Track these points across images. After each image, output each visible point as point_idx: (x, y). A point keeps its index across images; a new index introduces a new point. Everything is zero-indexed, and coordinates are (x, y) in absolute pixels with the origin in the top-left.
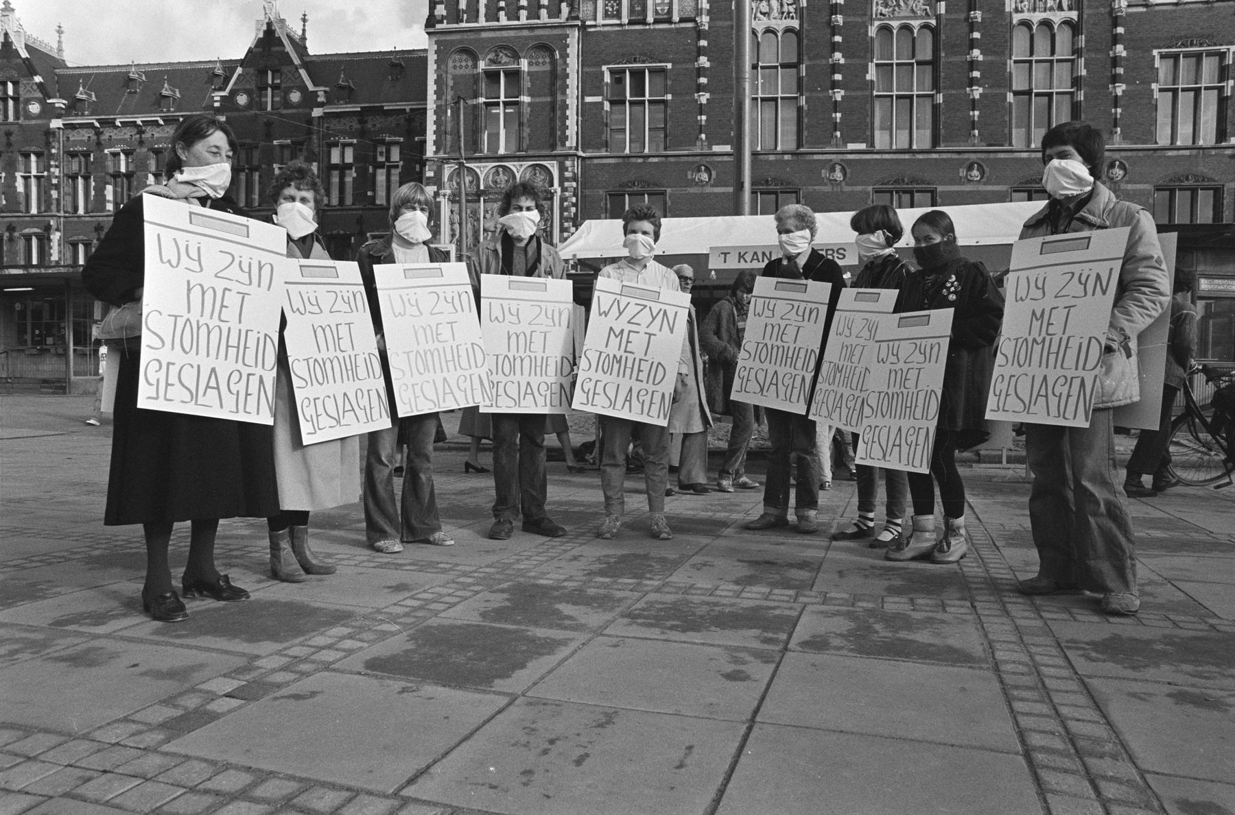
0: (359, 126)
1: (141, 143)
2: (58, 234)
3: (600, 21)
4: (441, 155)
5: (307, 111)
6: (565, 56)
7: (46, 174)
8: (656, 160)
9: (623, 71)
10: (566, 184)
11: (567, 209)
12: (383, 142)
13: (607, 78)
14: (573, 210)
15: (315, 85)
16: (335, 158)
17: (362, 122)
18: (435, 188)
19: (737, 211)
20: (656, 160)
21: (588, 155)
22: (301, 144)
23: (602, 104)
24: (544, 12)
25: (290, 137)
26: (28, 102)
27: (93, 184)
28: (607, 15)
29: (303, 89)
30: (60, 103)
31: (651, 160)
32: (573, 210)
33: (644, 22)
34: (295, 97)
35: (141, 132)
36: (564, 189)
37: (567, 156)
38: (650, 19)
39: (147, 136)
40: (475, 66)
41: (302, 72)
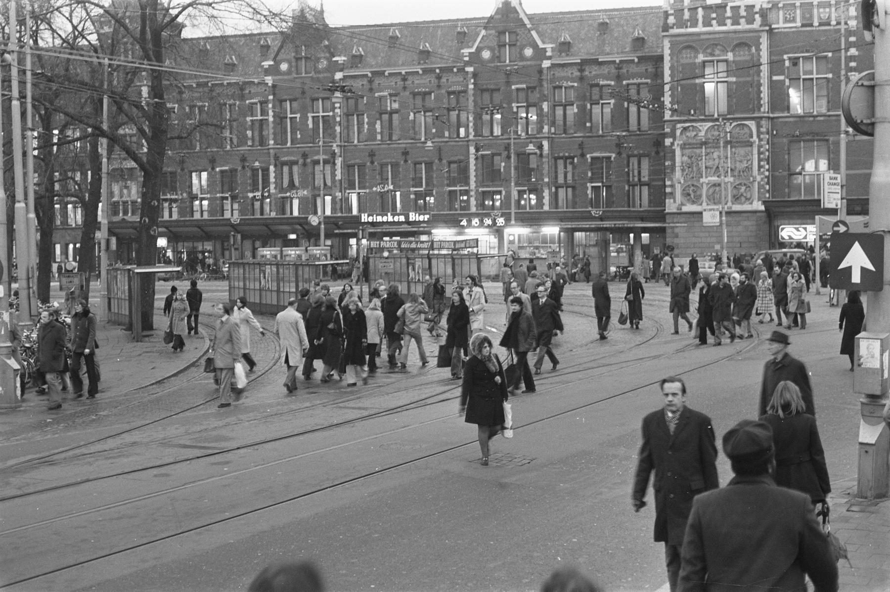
0: (578, 74)
1: (405, 88)
2: (340, 159)
3: (781, 25)
4: (675, 118)
5: (539, 62)
6: (758, 50)
7: (331, 114)
8: (822, 118)
9: (799, 58)
10: (762, 136)
11: (762, 153)
12: (597, 85)
13: (787, 63)
14: (767, 154)
15: (544, 43)
16: (561, 95)
17: (581, 71)
18: (671, 140)
19: (868, 199)
20: (822, 118)
21: (775, 115)
22: (535, 88)
23: (784, 81)
24: (742, 21)
25: (525, 82)
26: (318, 60)
27: (366, 120)
28: (786, 21)
29: (535, 46)
30: (340, 59)
31: (819, 118)
32: (767, 154)
33: (811, 25)
34: (528, 52)
35: (404, 80)
36: (760, 140)
37: (761, 118)
38: (816, 24)
39: (409, 82)
40: (696, 57)
41: (534, 33)
